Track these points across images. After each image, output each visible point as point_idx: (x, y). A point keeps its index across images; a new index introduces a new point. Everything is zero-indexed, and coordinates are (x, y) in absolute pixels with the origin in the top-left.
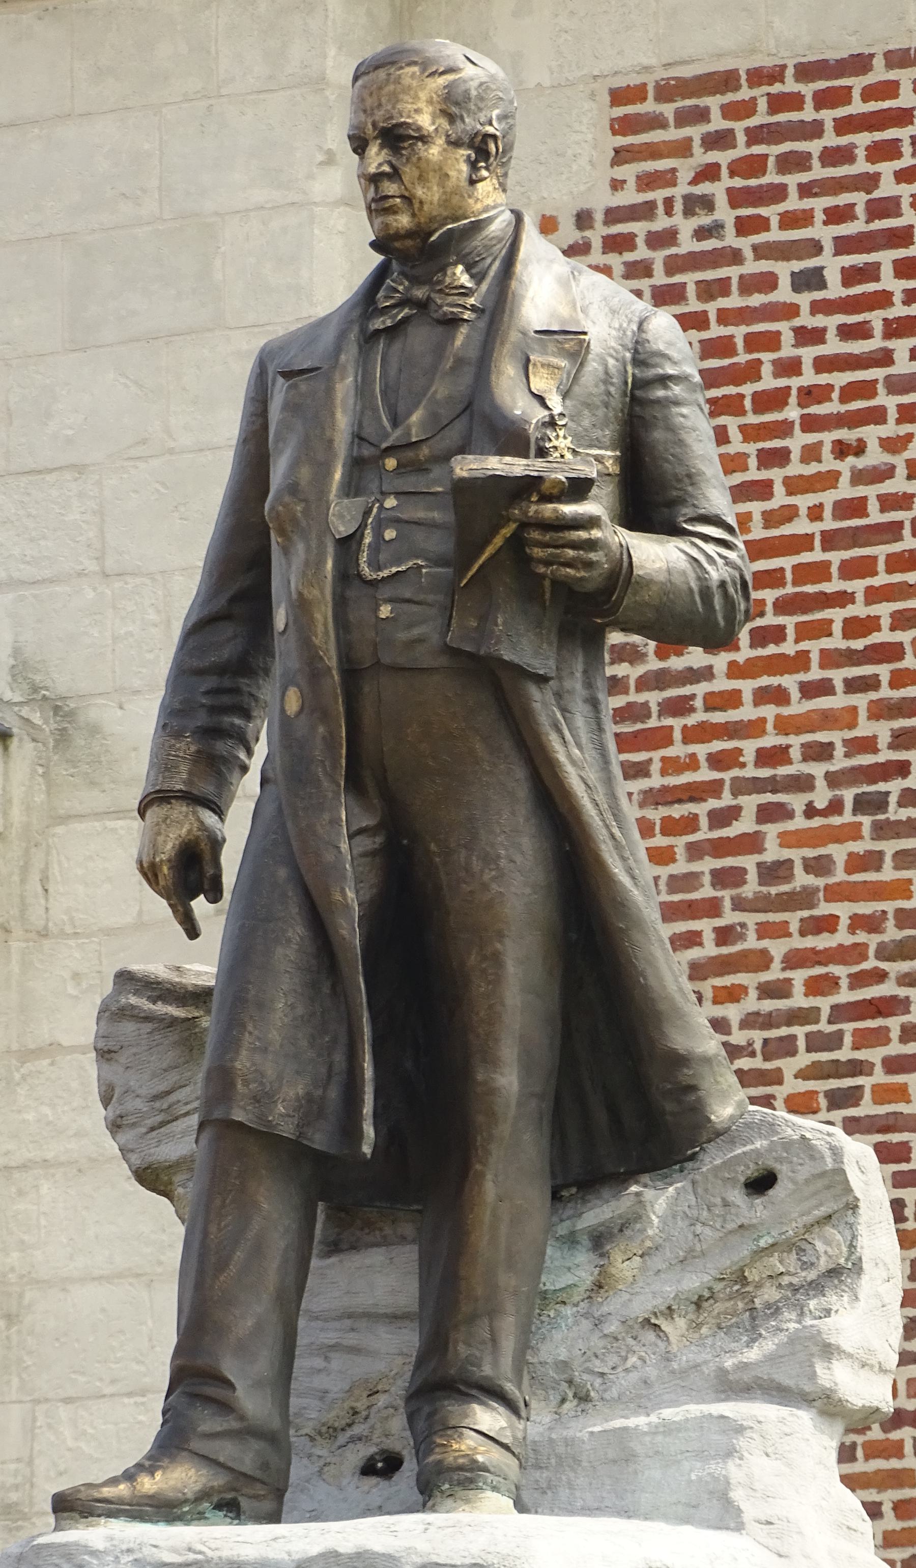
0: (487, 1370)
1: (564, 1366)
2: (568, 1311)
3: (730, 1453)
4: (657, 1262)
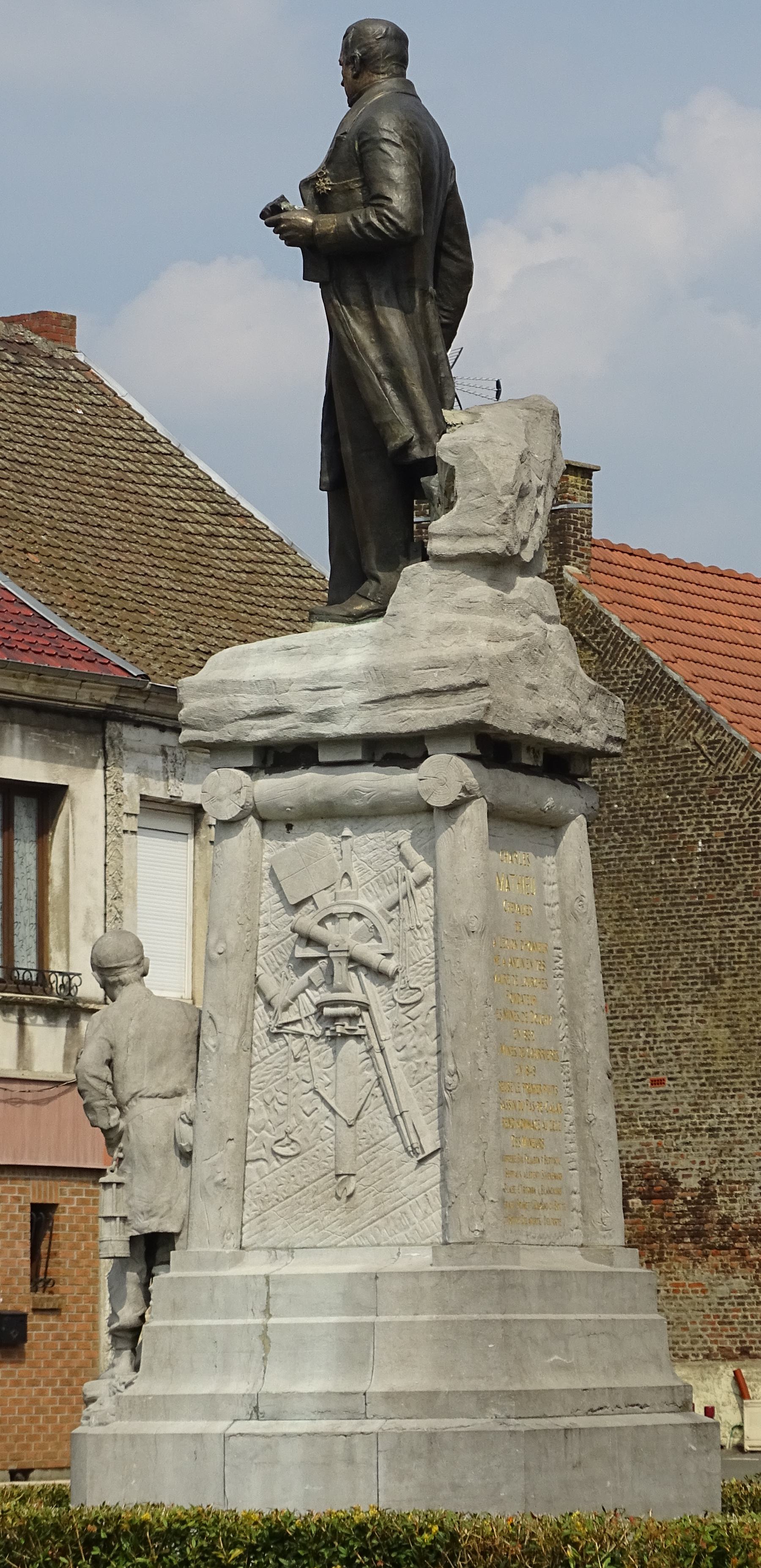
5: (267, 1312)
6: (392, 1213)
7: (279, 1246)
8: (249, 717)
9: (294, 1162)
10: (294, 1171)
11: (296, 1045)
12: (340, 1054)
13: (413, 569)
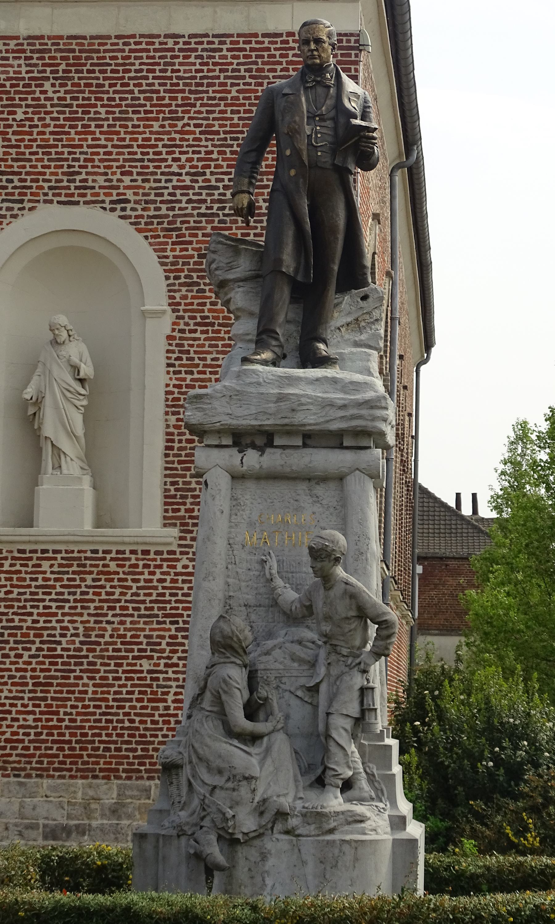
4: (342, 314)
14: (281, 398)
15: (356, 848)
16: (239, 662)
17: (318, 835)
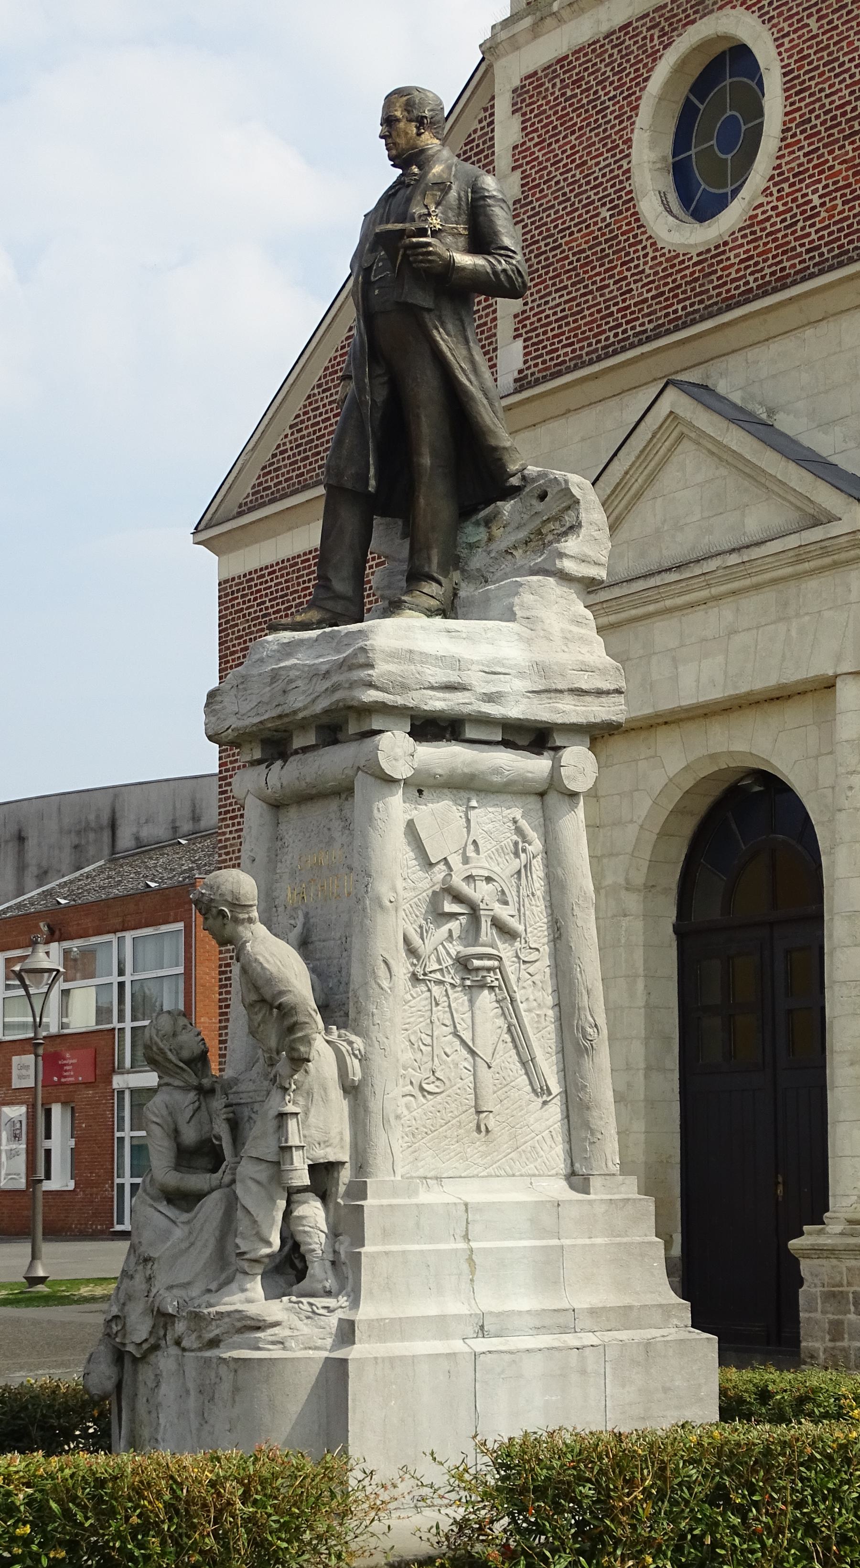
0: (427, 569)
1: (478, 570)
2: (480, 550)
3: (517, 593)
4: (508, 529)
5: (466, 1238)
6: (523, 1147)
7: (429, 1175)
8: (432, 688)
9: (439, 1097)
10: (440, 1107)
11: (437, 990)
12: (478, 1004)
13: (539, 581)
14: (275, 676)
15: (236, 1371)
16: (177, 1083)
17: (200, 1349)
